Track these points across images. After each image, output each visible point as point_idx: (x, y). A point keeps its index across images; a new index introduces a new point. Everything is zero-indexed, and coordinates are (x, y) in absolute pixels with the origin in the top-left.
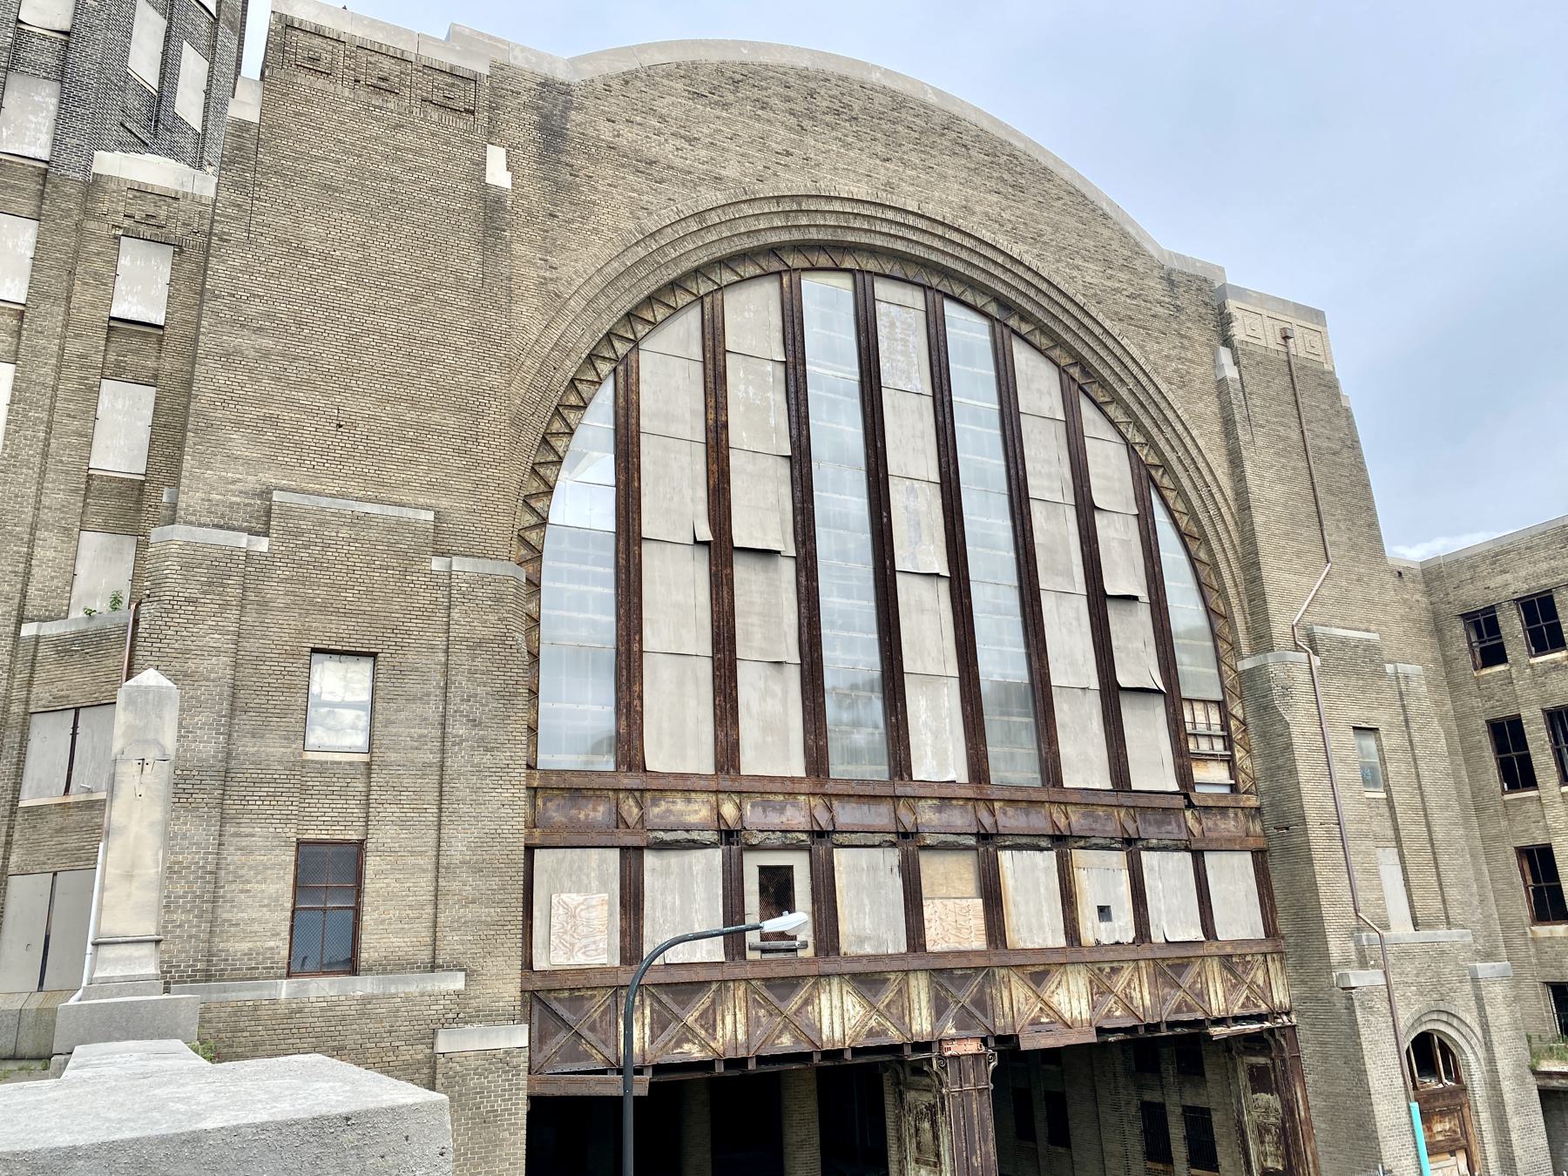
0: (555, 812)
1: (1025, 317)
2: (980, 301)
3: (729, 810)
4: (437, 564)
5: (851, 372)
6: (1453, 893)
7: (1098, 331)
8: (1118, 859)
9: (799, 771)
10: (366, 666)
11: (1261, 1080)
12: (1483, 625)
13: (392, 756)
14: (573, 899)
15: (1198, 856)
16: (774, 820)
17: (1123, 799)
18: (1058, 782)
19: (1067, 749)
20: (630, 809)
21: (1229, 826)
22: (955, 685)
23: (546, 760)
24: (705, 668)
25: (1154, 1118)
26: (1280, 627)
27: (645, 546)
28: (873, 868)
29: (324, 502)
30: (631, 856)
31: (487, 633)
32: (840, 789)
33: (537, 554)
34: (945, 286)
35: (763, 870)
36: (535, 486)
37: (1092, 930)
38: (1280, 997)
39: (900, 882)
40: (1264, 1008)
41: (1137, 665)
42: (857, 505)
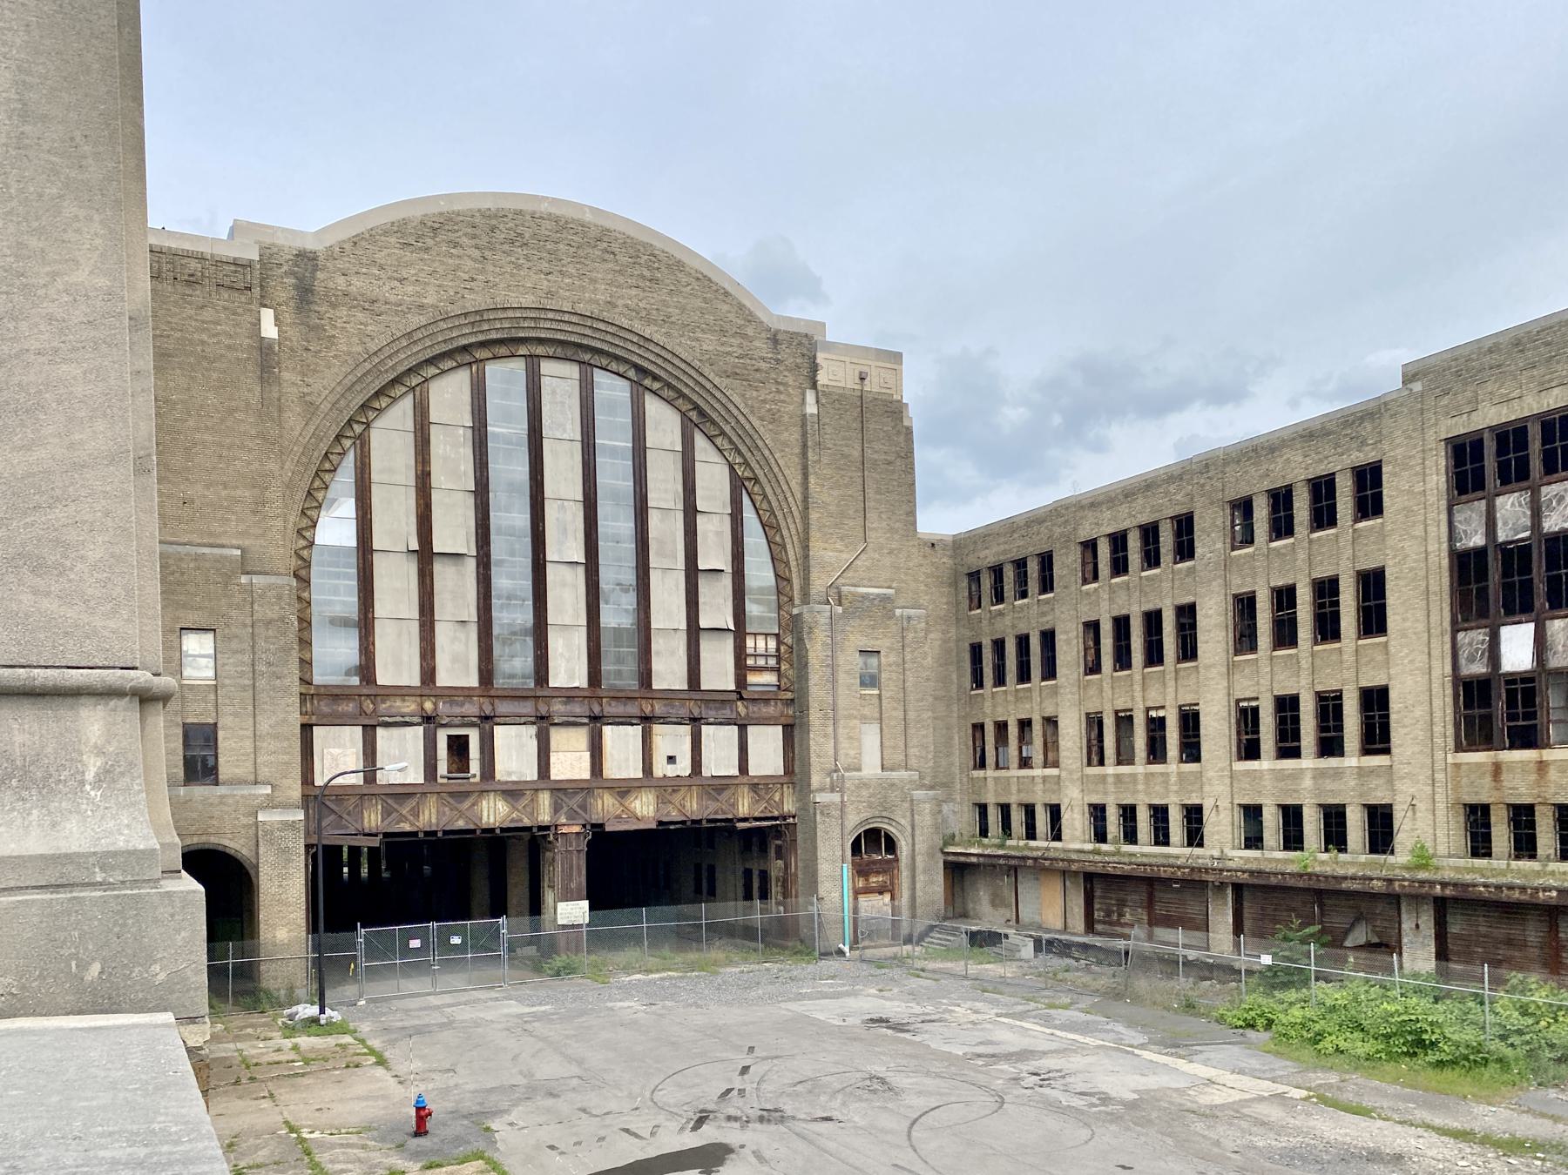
0: (325, 707)
1: (656, 378)
2: (622, 370)
3: (428, 706)
4: (244, 579)
5: (521, 428)
6: (913, 751)
7: (708, 386)
8: (685, 730)
9: (476, 684)
10: (210, 636)
11: (779, 856)
12: (974, 576)
13: (227, 682)
14: (336, 751)
15: (743, 729)
16: (457, 710)
17: (694, 695)
18: (650, 685)
19: (657, 665)
20: (368, 706)
21: (770, 710)
22: (584, 630)
23: (318, 679)
24: (415, 627)
25: (748, 874)
26: (819, 583)
27: (375, 555)
28: (519, 736)
29: (180, 548)
30: (369, 733)
31: (275, 616)
32: (500, 693)
33: (307, 564)
34: (596, 360)
35: (449, 737)
36: (305, 522)
37: (661, 768)
38: (789, 806)
39: (535, 743)
40: (776, 813)
41: (716, 610)
42: (522, 519)
